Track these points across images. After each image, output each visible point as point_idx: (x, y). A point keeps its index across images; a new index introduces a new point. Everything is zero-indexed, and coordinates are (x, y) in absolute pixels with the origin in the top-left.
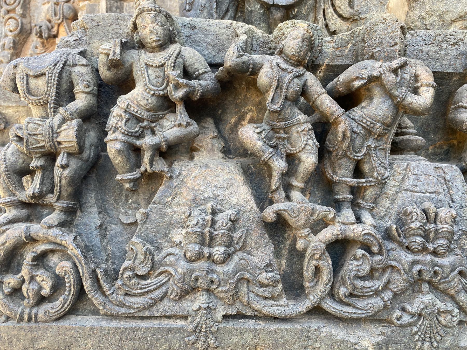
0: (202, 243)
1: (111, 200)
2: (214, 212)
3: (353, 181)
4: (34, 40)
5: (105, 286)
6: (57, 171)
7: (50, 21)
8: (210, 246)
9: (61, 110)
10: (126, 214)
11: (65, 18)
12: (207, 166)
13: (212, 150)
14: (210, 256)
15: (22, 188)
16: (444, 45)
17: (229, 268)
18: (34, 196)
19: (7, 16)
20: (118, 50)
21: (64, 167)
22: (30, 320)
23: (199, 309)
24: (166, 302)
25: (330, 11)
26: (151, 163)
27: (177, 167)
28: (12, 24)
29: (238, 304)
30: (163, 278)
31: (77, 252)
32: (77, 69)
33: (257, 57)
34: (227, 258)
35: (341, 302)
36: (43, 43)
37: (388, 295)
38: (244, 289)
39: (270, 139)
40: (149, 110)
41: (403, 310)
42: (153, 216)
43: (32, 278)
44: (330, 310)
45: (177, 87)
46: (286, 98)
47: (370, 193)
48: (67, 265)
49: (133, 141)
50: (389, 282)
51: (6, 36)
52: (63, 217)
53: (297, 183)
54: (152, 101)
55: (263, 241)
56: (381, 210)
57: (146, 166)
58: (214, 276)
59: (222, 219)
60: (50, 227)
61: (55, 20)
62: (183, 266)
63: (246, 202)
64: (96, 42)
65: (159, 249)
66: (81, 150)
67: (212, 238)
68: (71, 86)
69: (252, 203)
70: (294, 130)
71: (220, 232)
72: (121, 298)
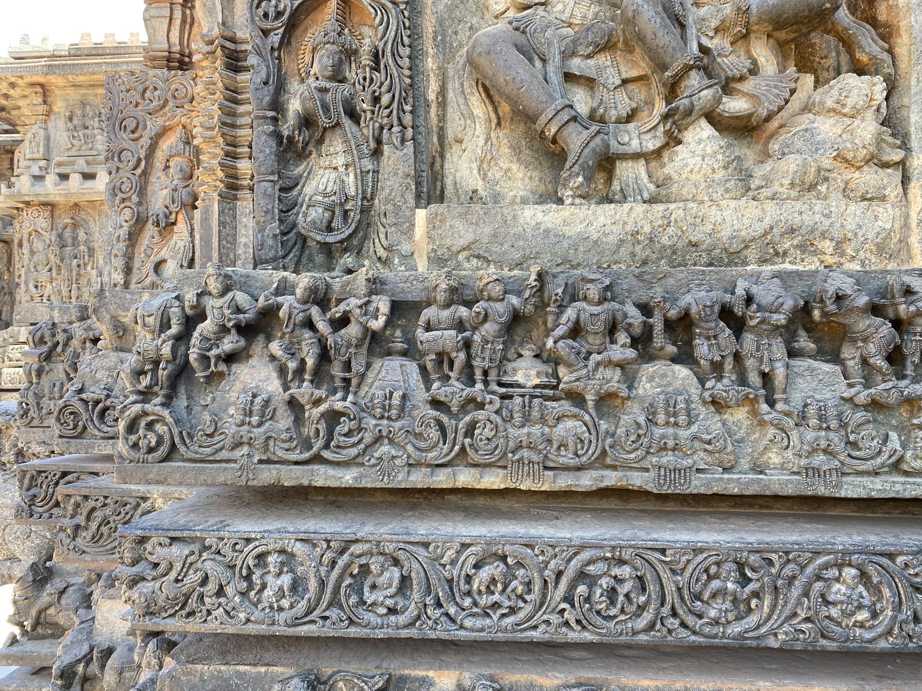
0: (245, 415)
1: (196, 391)
2: (254, 396)
3: (342, 375)
4: (150, 230)
5: (188, 441)
6: (160, 372)
7: (167, 208)
8: (250, 417)
9: (163, 335)
10: (204, 399)
11: (183, 205)
12: (254, 367)
13: (262, 356)
14: (249, 423)
15: (140, 383)
16: (415, 283)
17: (262, 430)
18: (146, 387)
19: (122, 206)
20: (195, 299)
21: (164, 369)
22: (143, 462)
23: (243, 455)
24: (223, 451)
25: (377, 241)
26: (216, 366)
27: (235, 367)
28: (127, 213)
29: (269, 454)
30: (222, 437)
31: (171, 420)
32: (173, 309)
33: (280, 299)
34: (260, 425)
35: (335, 452)
36: (160, 232)
37: (362, 446)
38: (271, 443)
39: (290, 349)
40: (214, 334)
41: (373, 456)
42: (217, 399)
43: (145, 436)
44: (325, 456)
45: (229, 320)
46: (295, 324)
47: (354, 382)
48: (166, 428)
49: (204, 352)
50: (362, 438)
51: (121, 226)
52: (164, 400)
53: (307, 377)
54: (216, 329)
55: (286, 414)
56: (362, 393)
57: (213, 368)
58: (252, 435)
59: (258, 400)
60: (155, 405)
61: (173, 208)
62: (234, 429)
63: (277, 389)
64: (186, 289)
65: (221, 419)
66: (174, 358)
67: (251, 412)
68: (169, 320)
69: (281, 390)
70: (304, 343)
71: (256, 408)
72: (196, 448)
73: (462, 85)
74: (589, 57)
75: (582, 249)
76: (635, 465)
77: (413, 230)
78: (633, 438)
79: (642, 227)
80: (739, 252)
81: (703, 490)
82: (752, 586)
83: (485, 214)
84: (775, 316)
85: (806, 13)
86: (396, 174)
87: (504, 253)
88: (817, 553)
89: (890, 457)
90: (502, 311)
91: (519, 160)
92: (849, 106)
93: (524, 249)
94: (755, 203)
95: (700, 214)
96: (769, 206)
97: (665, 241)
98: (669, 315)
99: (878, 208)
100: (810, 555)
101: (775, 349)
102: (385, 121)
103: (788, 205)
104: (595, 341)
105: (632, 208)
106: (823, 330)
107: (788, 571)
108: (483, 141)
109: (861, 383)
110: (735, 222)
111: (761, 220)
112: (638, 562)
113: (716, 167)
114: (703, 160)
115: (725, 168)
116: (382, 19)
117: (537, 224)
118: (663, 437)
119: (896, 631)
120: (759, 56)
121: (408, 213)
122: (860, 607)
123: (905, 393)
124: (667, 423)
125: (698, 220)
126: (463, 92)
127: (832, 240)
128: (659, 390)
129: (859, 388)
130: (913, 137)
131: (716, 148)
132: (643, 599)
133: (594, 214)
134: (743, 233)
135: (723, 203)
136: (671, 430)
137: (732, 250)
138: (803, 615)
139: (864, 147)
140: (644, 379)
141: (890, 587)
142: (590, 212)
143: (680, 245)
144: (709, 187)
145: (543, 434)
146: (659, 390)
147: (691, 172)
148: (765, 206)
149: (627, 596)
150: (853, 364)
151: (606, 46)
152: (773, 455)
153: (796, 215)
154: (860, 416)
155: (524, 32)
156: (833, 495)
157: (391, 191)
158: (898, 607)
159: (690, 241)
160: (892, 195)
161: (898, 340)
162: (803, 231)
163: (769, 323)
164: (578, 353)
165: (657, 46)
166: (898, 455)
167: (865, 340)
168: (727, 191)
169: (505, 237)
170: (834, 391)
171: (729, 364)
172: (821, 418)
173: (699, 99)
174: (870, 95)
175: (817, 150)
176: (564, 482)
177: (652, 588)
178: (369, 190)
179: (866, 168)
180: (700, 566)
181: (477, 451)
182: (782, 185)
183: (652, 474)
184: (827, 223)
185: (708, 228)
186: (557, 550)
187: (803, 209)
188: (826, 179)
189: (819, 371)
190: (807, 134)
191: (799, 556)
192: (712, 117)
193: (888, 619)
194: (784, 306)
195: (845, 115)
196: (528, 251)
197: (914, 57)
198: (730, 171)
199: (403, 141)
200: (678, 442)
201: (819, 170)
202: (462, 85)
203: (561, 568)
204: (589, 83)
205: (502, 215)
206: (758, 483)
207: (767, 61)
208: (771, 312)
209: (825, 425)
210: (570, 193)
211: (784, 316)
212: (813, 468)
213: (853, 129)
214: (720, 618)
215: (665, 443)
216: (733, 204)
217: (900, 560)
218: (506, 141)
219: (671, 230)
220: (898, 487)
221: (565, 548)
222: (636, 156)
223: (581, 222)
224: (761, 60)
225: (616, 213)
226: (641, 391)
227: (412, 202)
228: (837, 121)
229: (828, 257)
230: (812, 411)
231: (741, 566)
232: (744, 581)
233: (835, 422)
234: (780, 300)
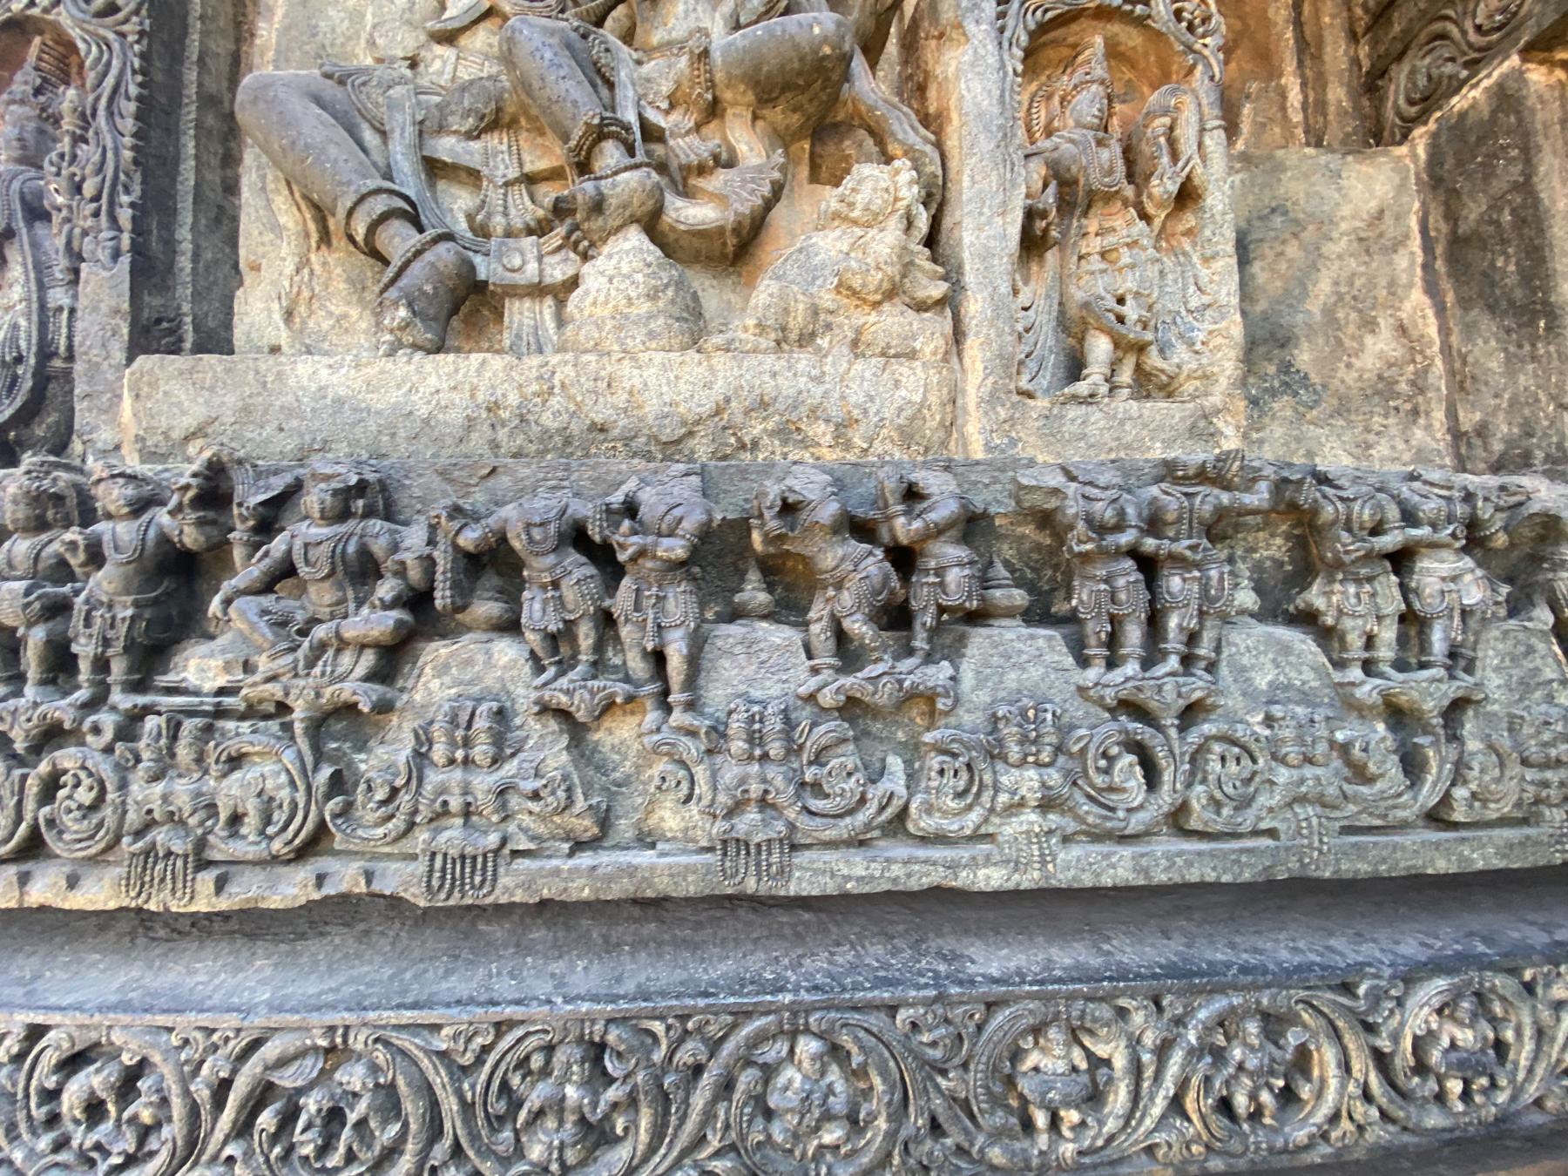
73: (263, 178)
74: (470, 136)
75: (402, 433)
76: (387, 849)
77: (118, 405)
78: (380, 795)
79: (504, 395)
80: (679, 441)
81: (518, 897)
82: (613, 1094)
83: (228, 371)
84: (666, 542)
85: (796, 65)
86: (96, 309)
87: (267, 441)
88: (743, 1014)
89: (882, 809)
90: (126, 538)
91: (361, 300)
92: (859, 206)
93: (301, 435)
94: (697, 356)
95: (603, 373)
96: (720, 361)
97: (547, 420)
98: (461, 541)
99: (902, 369)
100: (729, 1019)
101: (671, 604)
102: (90, 222)
103: (751, 361)
104: (321, 596)
105: (484, 362)
106: (795, 569)
107: (684, 1056)
108: (292, 267)
109: (831, 667)
110: (665, 389)
111: (708, 386)
112: (381, 1055)
113: (633, 294)
114: (610, 281)
115: (652, 296)
116: (99, 59)
117: (321, 388)
118: (442, 790)
119: (896, 1160)
120: (738, 142)
121: (110, 376)
122: (827, 1117)
123: (907, 684)
124: (452, 761)
125: (603, 385)
126: (263, 189)
127: (827, 421)
128: (454, 691)
129: (826, 675)
130: (967, 267)
131: (638, 265)
132: (394, 1129)
133: (418, 371)
134: (681, 409)
135: (644, 357)
136: (457, 774)
137: (664, 439)
138: (714, 1143)
139: (878, 268)
140: (428, 670)
141: (884, 1074)
142: (412, 367)
143: (575, 428)
144: (620, 328)
145: (198, 794)
146: (454, 691)
147: (594, 303)
148: (714, 362)
149: (362, 1124)
150: (819, 630)
151: (494, 122)
152: (667, 814)
153: (766, 378)
154: (827, 730)
155: (341, 82)
156: (773, 892)
157: (84, 339)
158: (899, 1111)
159: (593, 424)
160: (928, 350)
161: (895, 582)
162: (780, 406)
163: (654, 557)
164: (283, 624)
165: (549, 99)
166: (897, 804)
167: (839, 586)
168: (652, 335)
169: (266, 412)
170: (785, 682)
171: (586, 636)
172: (755, 738)
173: (614, 185)
174: (892, 190)
175: (815, 278)
176: (245, 891)
177: (412, 1108)
178: (63, 342)
179: (886, 307)
180: (508, 1057)
181: (61, 832)
182: (746, 329)
183: (421, 867)
184: (818, 391)
185: (621, 399)
186: (215, 1037)
187: (777, 368)
188: (828, 327)
189: (762, 645)
190: (802, 257)
191: (708, 1022)
192: (652, 224)
193: (880, 1139)
194: (685, 524)
195: (855, 222)
196: (308, 438)
197: (966, 144)
198: (661, 304)
199: (116, 255)
200: (470, 799)
201: (815, 311)
202: (263, 178)
203: (223, 1074)
204: (473, 177)
205: (257, 373)
206: (631, 876)
207: (751, 150)
208: (659, 534)
209: (758, 752)
210: (388, 337)
211: (683, 542)
212: (738, 840)
213: (866, 244)
214: (549, 1161)
215: (445, 803)
216: (659, 357)
217: (903, 1015)
218: (339, 270)
219: (556, 402)
220: (897, 870)
221: (231, 1035)
222: (538, 290)
223: (399, 387)
224: (742, 148)
225: (457, 371)
226: (418, 697)
227: (119, 356)
228: (844, 233)
229: (825, 450)
230: (736, 726)
231: (596, 1051)
232: (599, 1077)
233: (777, 744)
234: (677, 512)
